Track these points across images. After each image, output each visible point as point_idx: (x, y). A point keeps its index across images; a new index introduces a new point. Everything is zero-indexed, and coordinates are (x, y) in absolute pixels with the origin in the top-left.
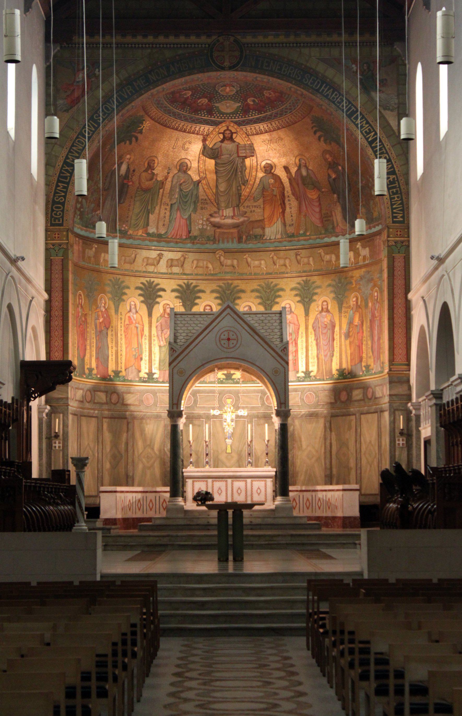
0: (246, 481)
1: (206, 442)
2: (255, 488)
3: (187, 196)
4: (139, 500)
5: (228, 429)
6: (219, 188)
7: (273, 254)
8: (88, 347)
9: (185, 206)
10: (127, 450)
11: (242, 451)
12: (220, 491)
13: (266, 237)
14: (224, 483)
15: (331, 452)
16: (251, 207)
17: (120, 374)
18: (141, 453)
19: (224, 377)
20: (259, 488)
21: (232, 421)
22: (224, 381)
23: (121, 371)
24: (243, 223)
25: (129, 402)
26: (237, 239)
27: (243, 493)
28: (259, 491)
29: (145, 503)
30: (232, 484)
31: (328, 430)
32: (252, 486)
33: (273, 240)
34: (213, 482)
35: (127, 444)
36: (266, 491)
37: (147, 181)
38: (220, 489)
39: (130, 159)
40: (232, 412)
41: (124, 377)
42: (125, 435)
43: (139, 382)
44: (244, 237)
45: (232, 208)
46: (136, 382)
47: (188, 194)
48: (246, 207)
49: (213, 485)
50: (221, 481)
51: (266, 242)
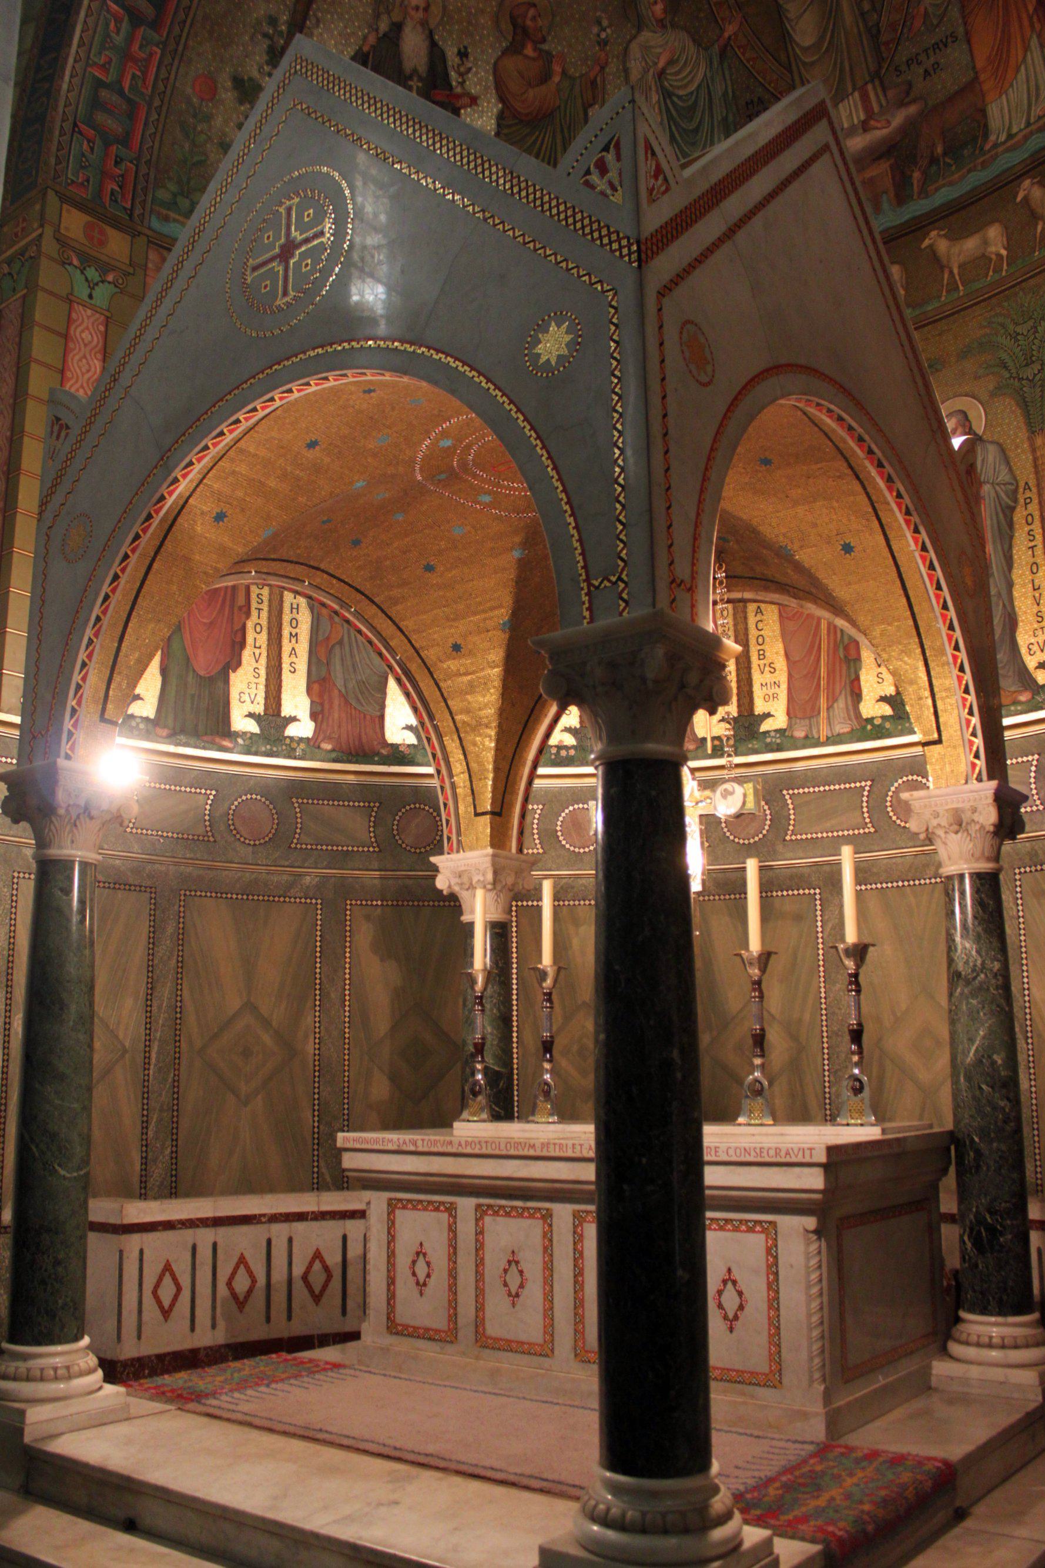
3: (693, 108)
6: (797, 38)
7: (1027, 183)
8: (256, 638)
9: (694, 144)
12: (514, 1281)
13: (993, 138)
14: (534, 1228)
16: (922, 57)
19: (887, 710)
22: (887, 725)
24: (910, 129)
26: (892, 194)
33: (1019, 137)
34: (481, 1212)
36: (774, 1302)
37: (530, 85)
39: (426, 9)
44: (916, 175)
45: (856, 94)
47: (696, 101)
48: (903, 68)
49: (480, 1233)
51: (994, 158)
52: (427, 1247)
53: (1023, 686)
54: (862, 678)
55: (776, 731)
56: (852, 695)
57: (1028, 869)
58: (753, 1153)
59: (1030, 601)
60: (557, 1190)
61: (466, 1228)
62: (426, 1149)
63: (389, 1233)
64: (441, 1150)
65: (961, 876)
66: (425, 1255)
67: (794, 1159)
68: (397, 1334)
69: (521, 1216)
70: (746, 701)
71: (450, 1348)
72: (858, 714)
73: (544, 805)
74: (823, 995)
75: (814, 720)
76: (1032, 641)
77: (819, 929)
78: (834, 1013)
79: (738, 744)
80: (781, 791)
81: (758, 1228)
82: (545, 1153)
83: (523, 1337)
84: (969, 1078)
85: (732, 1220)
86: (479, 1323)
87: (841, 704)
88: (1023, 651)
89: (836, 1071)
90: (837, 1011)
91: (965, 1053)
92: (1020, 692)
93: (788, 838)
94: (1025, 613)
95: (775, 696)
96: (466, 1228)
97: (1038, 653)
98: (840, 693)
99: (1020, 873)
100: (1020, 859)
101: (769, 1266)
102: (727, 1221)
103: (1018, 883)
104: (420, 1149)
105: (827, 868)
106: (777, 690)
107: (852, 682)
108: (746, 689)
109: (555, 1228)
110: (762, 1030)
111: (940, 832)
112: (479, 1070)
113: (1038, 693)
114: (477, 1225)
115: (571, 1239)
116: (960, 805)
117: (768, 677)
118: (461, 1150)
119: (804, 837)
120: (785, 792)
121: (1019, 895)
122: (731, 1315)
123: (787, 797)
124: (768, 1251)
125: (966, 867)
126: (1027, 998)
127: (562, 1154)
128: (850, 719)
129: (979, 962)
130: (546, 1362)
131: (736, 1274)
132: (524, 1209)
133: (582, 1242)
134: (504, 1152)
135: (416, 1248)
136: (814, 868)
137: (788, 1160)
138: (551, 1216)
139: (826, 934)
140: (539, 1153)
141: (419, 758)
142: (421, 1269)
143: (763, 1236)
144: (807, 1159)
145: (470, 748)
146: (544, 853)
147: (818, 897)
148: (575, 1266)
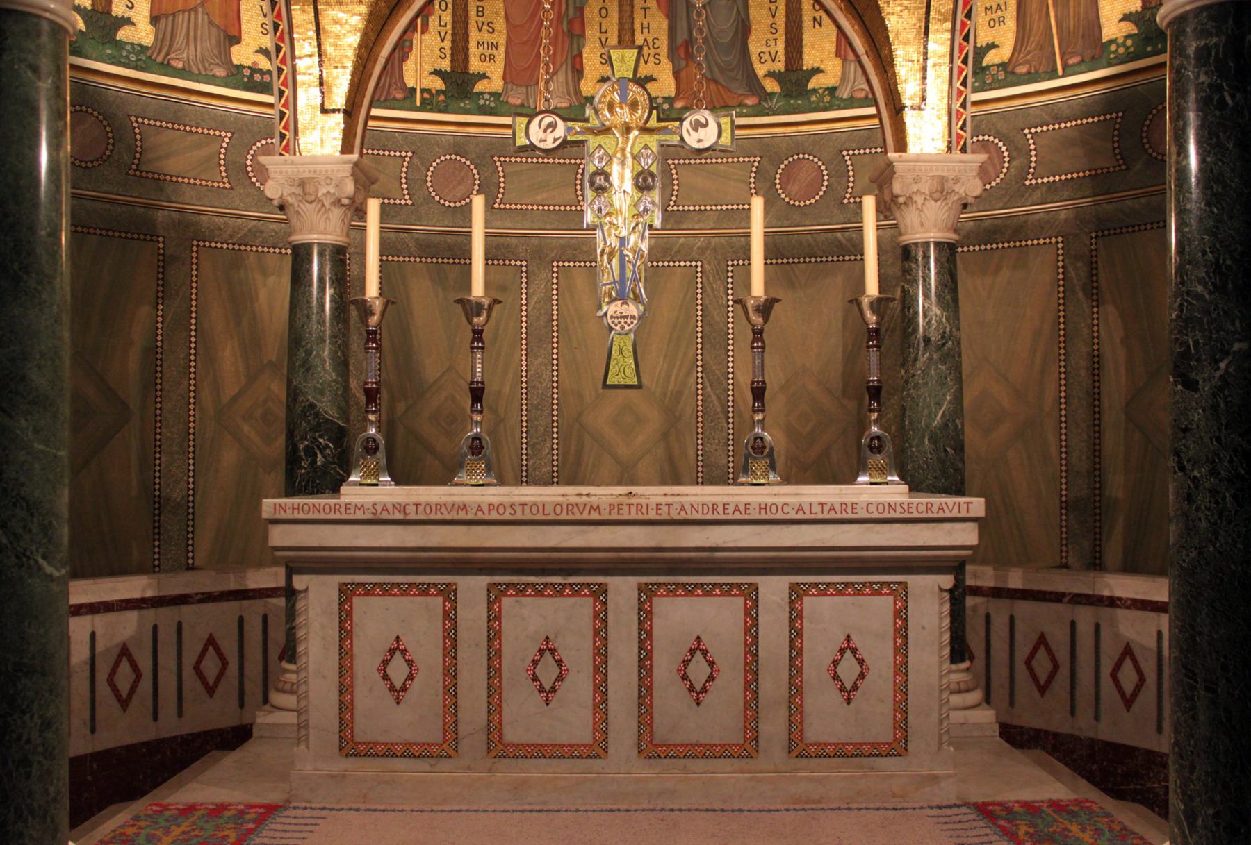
0: (752, 596)
1: (471, 309)
2: (819, 650)
4: (124, 652)
5: (624, 233)
10: (151, 382)
11: (679, 394)
12: (547, 673)
14: (584, 607)
15: (1095, 395)
17: (123, 34)
18: (235, 398)
20: (848, 647)
21: (643, 183)
23: (128, 21)
25: (171, 166)
27: (730, 683)
28: (848, 669)
29: (167, 660)
30: (645, 616)
31: (1080, 295)
32: (795, 634)
34: (495, 595)
35: (153, 354)
38: (547, 648)
40: (645, 130)
41: (144, 48)
42: (144, 311)
43: (226, 86)
46: (212, 80)
49: (494, 618)
50: (559, 592)
52: (406, 642)
53: (750, 90)
54: (585, 55)
55: (491, 94)
56: (573, 72)
57: (741, 262)
58: (899, 509)
59: (765, 12)
60: (624, 561)
61: (472, 613)
62: (422, 517)
63: (341, 628)
64: (447, 517)
65: (927, 244)
66: (404, 652)
67: (948, 515)
68: (357, 755)
69: (560, 594)
70: (461, 57)
71: (445, 764)
72: (578, 92)
73: (233, 133)
74: (524, 368)
75: (531, 90)
76: (764, 50)
77: (524, 302)
78: (534, 387)
79: (449, 101)
80: (492, 157)
81: (885, 590)
82: (614, 516)
83: (563, 739)
84: (933, 440)
85: (853, 584)
86: (494, 727)
87: (561, 77)
88: (754, 58)
89: (534, 445)
90: (537, 384)
91: (931, 417)
92: (747, 96)
93: (496, 206)
94: (759, 22)
95: (492, 58)
96: (472, 613)
97: (770, 62)
98: (561, 65)
99: (733, 265)
100: (734, 252)
101: (897, 630)
102: (846, 584)
103: (730, 274)
104: (412, 516)
105: (536, 241)
106: (494, 51)
107: (574, 58)
108: (461, 44)
109: (610, 605)
110: (764, 382)
111: (919, 199)
112: (371, 422)
113: (766, 100)
114: (489, 609)
115: (636, 618)
116: (945, 174)
117: (485, 36)
118: (480, 516)
119: (513, 207)
120: (496, 158)
121: (730, 286)
122: (848, 686)
123: (498, 164)
124: (897, 614)
125: (933, 235)
126: (731, 381)
127: (640, 517)
128: (569, 94)
129: (948, 329)
130: (596, 764)
131: (857, 641)
132: (564, 585)
133: (651, 620)
134: (552, 517)
135: (390, 644)
136: (521, 239)
137: (941, 515)
138: (606, 592)
139: (531, 307)
140: (605, 516)
141: (88, 49)
142: (398, 671)
143: (891, 598)
144: (963, 514)
145: (324, 22)
146: (231, 188)
147: (524, 269)
148: (640, 648)
